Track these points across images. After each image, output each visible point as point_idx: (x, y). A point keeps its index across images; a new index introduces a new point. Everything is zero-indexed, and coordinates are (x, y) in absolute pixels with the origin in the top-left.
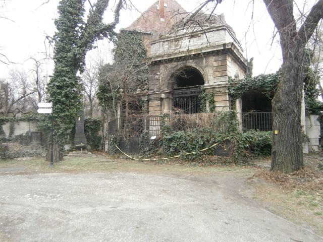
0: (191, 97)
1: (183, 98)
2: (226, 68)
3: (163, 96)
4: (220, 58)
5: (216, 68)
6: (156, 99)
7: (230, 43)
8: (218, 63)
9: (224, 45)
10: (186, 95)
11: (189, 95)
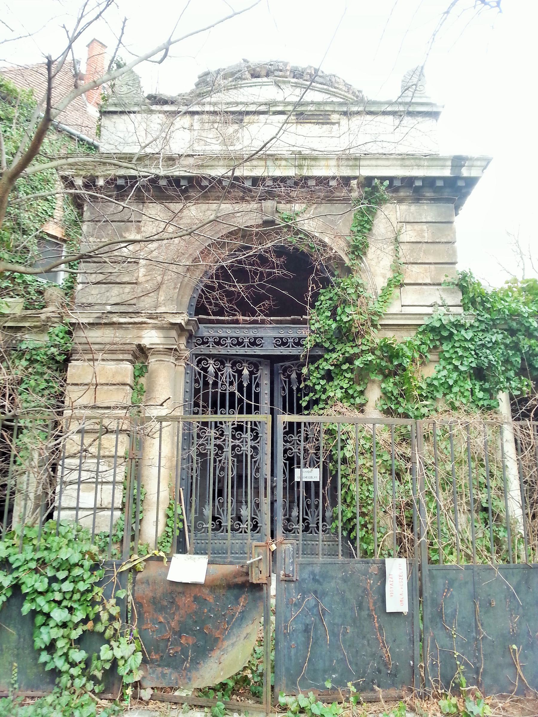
0: (272, 360)
1: (236, 361)
2: (454, 253)
3: (151, 338)
4: (427, 212)
5: (412, 251)
6: (112, 351)
9: (458, 162)
10: (258, 351)
11: (269, 349)
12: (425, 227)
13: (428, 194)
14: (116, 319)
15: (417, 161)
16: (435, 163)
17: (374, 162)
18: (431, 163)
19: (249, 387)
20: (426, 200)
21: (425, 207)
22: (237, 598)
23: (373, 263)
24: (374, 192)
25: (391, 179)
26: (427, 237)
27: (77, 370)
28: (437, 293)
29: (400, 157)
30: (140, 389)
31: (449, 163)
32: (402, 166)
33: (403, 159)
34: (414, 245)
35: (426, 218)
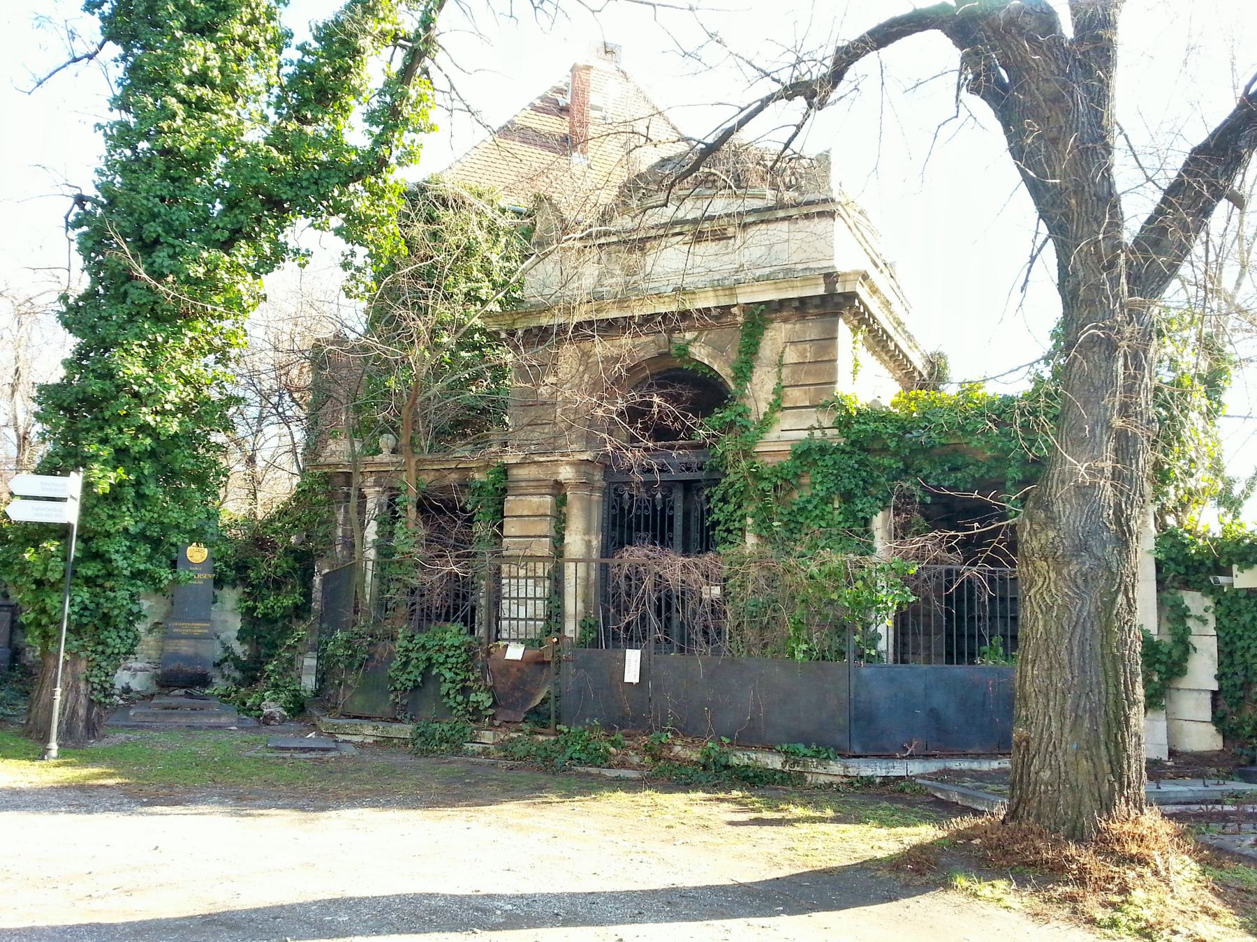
3: (566, 473)
4: (812, 330)
5: (794, 373)
6: (538, 486)
7: (856, 273)
8: (803, 354)
14: (537, 458)
19: (663, 510)
22: (542, 670)
23: (757, 388)
24: (759, 317)
26: (809, 357)
27: (512, 504)
28: (815, 416)
30: (560, 521)
31: (822, 281)
34: (796, 367)
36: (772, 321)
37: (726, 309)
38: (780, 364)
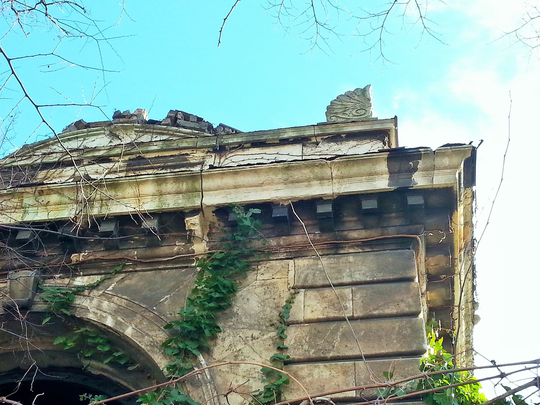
12: (347, 291)
13: (354, 235)
15: (317, 170)
16: (355, 170)
17: (229, 181)
18: (345, 171)
20: (352, 247)
21: (351, 259)
25: (267, 206)
29: (279, 165)
31: (383, 167)
32: (287, 182)
33: (288, 168)
35: (351, 276)
36: (267, 254)
37: (172, 221)
38: (283, 322)
